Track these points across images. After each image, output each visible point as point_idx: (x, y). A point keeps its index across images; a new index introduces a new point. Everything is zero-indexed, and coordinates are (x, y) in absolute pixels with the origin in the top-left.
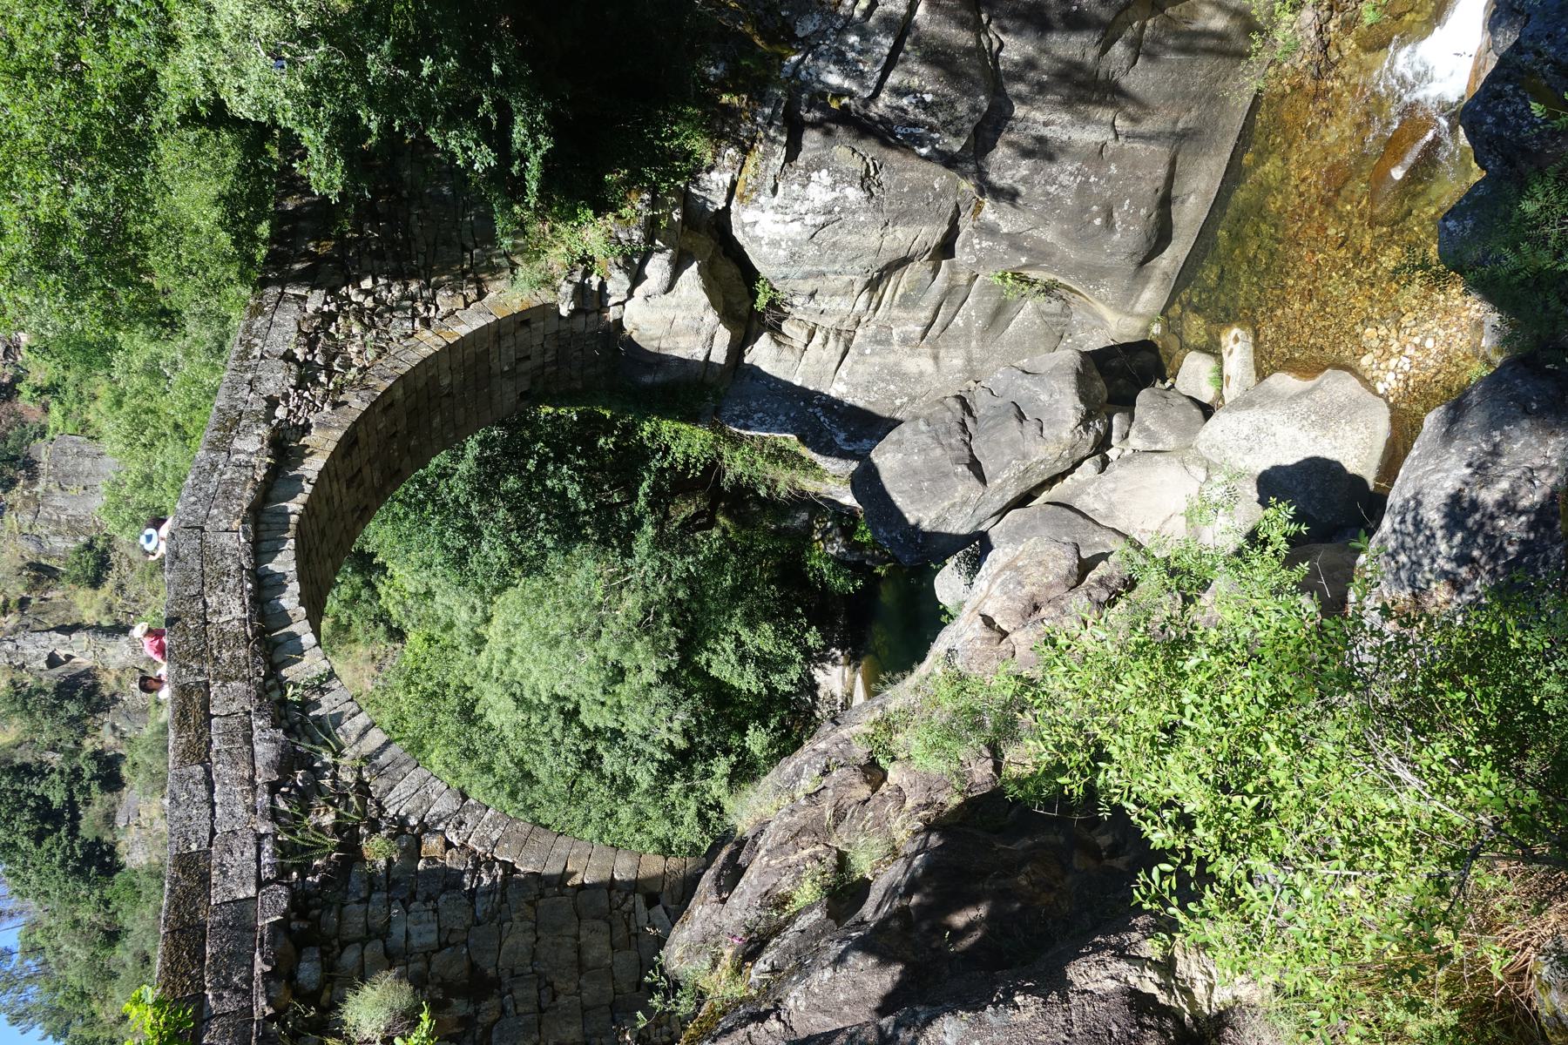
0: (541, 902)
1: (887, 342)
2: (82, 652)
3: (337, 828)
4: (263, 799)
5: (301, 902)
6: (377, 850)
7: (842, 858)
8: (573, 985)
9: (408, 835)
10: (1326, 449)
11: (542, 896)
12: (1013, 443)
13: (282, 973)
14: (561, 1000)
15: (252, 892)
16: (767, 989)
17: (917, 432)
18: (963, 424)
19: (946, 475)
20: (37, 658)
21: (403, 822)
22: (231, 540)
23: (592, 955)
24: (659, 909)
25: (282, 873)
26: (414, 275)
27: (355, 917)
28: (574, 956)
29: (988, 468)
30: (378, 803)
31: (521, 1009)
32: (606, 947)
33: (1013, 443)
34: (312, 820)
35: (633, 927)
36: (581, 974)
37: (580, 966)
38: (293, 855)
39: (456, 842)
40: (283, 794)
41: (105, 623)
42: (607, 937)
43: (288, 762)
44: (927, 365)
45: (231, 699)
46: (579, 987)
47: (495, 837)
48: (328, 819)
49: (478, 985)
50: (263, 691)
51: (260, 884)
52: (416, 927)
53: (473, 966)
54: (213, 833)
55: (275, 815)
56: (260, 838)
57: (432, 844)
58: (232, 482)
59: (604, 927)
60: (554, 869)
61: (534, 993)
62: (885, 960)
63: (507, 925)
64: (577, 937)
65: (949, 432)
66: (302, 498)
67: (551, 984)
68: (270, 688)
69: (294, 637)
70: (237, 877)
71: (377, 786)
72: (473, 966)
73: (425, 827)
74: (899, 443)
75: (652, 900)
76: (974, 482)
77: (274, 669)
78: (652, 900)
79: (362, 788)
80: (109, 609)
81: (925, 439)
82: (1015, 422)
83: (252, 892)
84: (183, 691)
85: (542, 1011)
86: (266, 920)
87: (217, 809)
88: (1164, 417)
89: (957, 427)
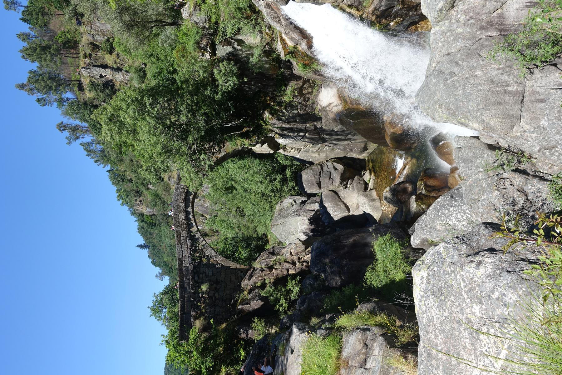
1: (308, 152)
2: (109, 74)
3: (199, 256)
5: (195, 267)
6: (204, 260)
7: (265, 280)
9: (209, 258)
10: (372, 213)
12: (327, 183)
13: (193, 278)
16: (250, 299)
17: (310, 172)
18: (320, 173)
19: (313, 184)
20: (97, 75)
21: (208, 256)
22: (182, 204)
25: (192, 263)
26: (211, 141)
27: (202, 269)
29: (322, 186)
33: (327, 183)
34: (195, 255)
38: (193, 260)
41: (115, 67)
43: (192, 246)
44: (317, 155)
45: (183, 234)
48: (198, 255)
49: (217, 282)
52: (209, 272)
53: (217, 279)
55: (191, 254)
57: (212, 260)
58: (181, 192)
60: (228, 265)
62: (262, 301)
65: (316, 174)
66: (192, 196)
68: (189, 232)
69: (192, 223)
70: (187, 262)
71: (204, 250)
72: (217, 279)
73: (211, 257)
74: (307, 173)
75: (242, 272)
76: (318, 188)
77: (189, 229)
78: (242, 272)
79: (202, 250)
80: (115, 62)
81: (312, 174)
82: (328, 179)
84: (177, 231)
86: (190, 270)
88: (357, 185)
89: (318, 174)
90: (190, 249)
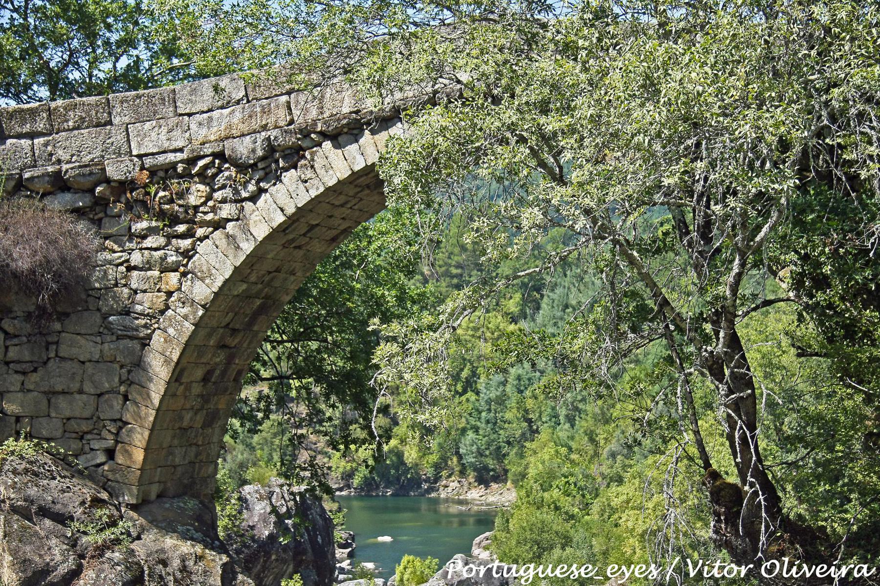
0: (117, 366)
4: (208, 150)
8: (32, 387)
11: (122, 367)
14: (20, 378)
15: (135, 153)
23: (62, 403)
24: (101, 458)
28: (59, 388)
30: (207, 237)
31: (11, 349)
32: (68, 414)
35: (89, 437)
36: (44, 393)
37: (51, 394)
39: (172, 299)
40: (213, 162)
42: (78, 415)
46: (29, 391)
47: (171, 331)
50: (305, 133)
51: (140, 156)
54: (189, 115)
55: (191, 162)
56: (181, 150)
59: (87, 413)
61: (27, 359)
63: (98, 339)
64: (81, 392)
67: (35, 370)
83: (135, 153)
85: (7, 363)
87: (205, 115)
90: (220, 155)
